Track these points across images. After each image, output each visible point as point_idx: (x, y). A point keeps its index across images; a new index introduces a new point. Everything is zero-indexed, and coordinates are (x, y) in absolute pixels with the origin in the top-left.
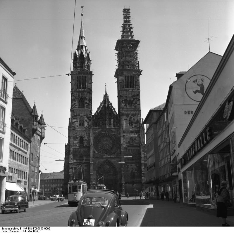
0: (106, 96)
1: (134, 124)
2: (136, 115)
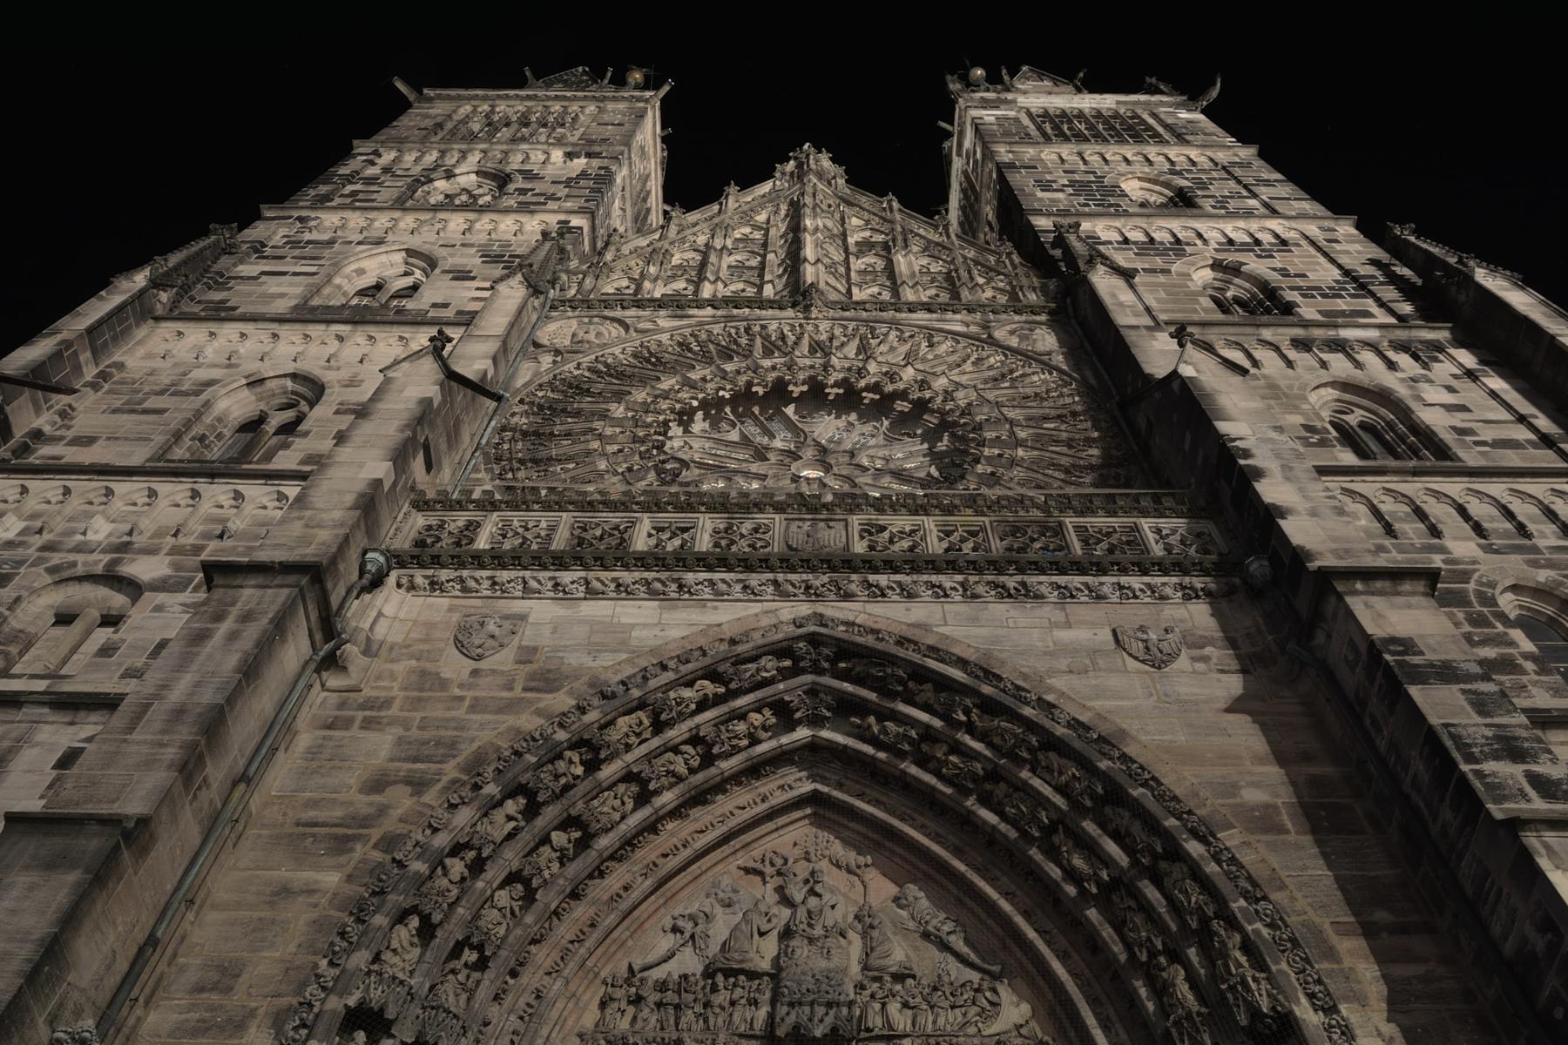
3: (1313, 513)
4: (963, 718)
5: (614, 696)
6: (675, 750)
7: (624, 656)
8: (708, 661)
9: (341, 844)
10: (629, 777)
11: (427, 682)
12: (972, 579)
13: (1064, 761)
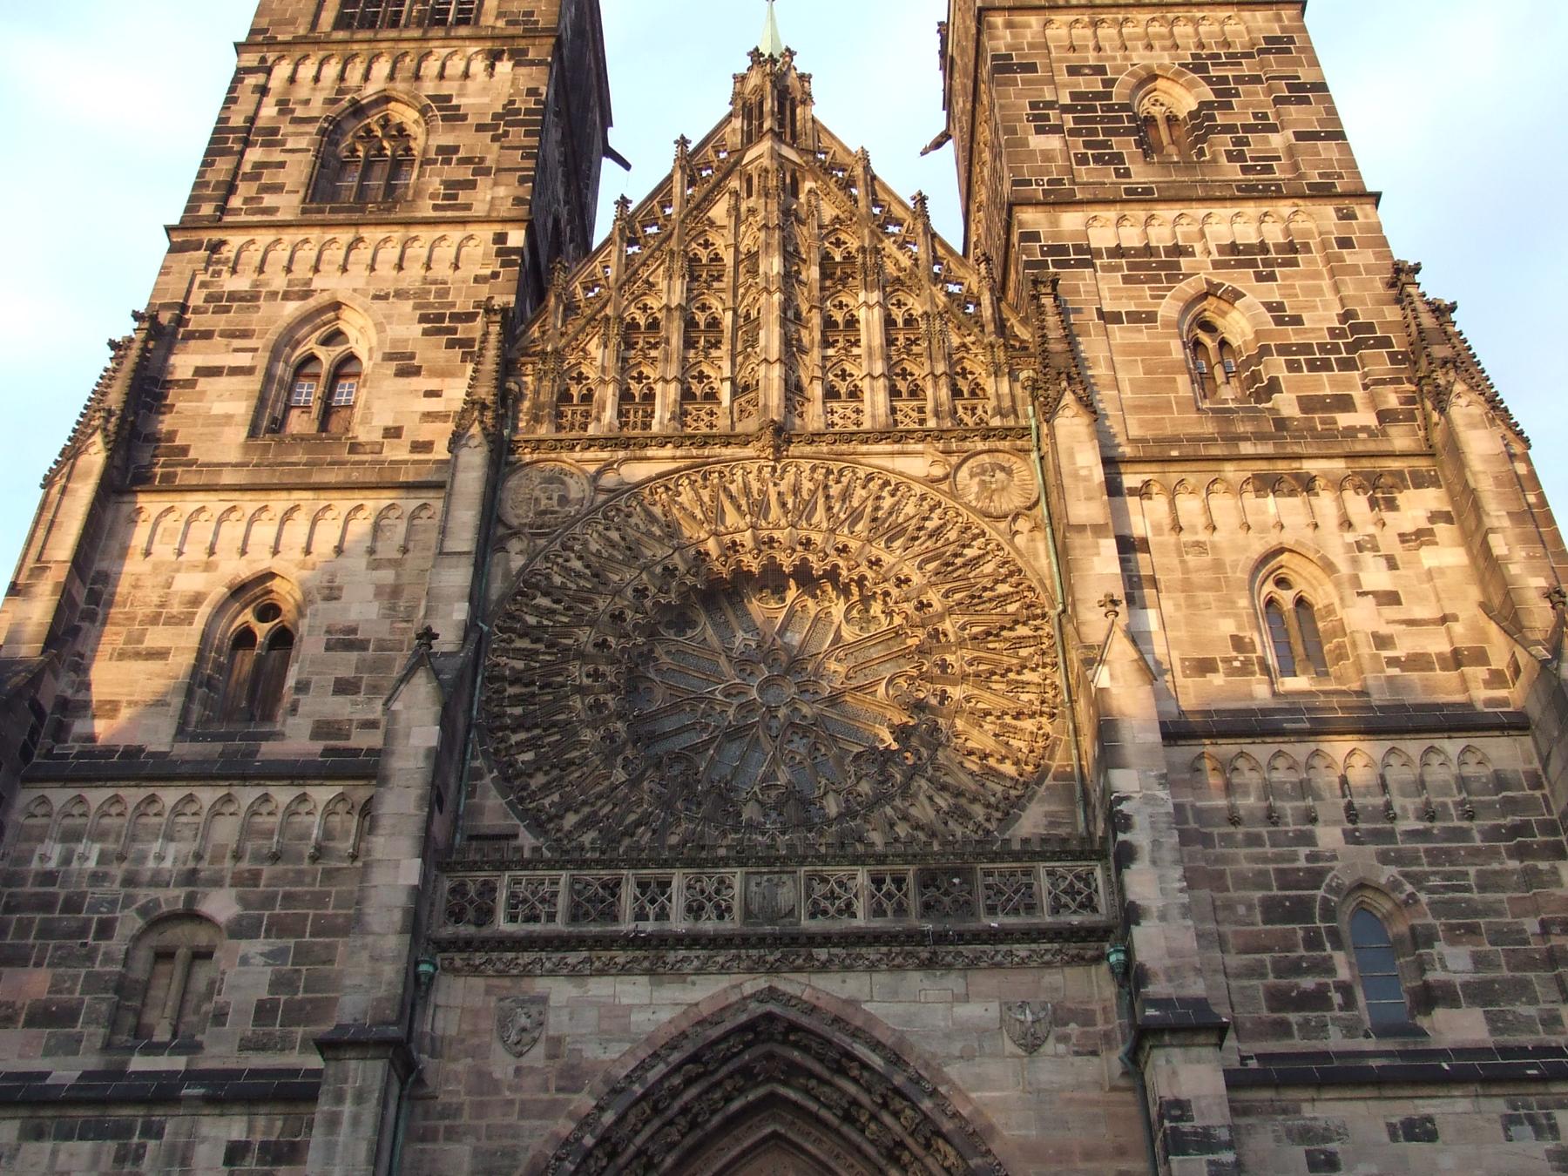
1: (1293, 367)
3: (1163, 917)
4: (880, 1101)
5: (623, 1090)
6: (671, 1123)
7: (627, 1046)
8: (689, 1048)
10: (640, 1153)
11: (483, 1082)
12: (896, 949)
13: (948, 1149)
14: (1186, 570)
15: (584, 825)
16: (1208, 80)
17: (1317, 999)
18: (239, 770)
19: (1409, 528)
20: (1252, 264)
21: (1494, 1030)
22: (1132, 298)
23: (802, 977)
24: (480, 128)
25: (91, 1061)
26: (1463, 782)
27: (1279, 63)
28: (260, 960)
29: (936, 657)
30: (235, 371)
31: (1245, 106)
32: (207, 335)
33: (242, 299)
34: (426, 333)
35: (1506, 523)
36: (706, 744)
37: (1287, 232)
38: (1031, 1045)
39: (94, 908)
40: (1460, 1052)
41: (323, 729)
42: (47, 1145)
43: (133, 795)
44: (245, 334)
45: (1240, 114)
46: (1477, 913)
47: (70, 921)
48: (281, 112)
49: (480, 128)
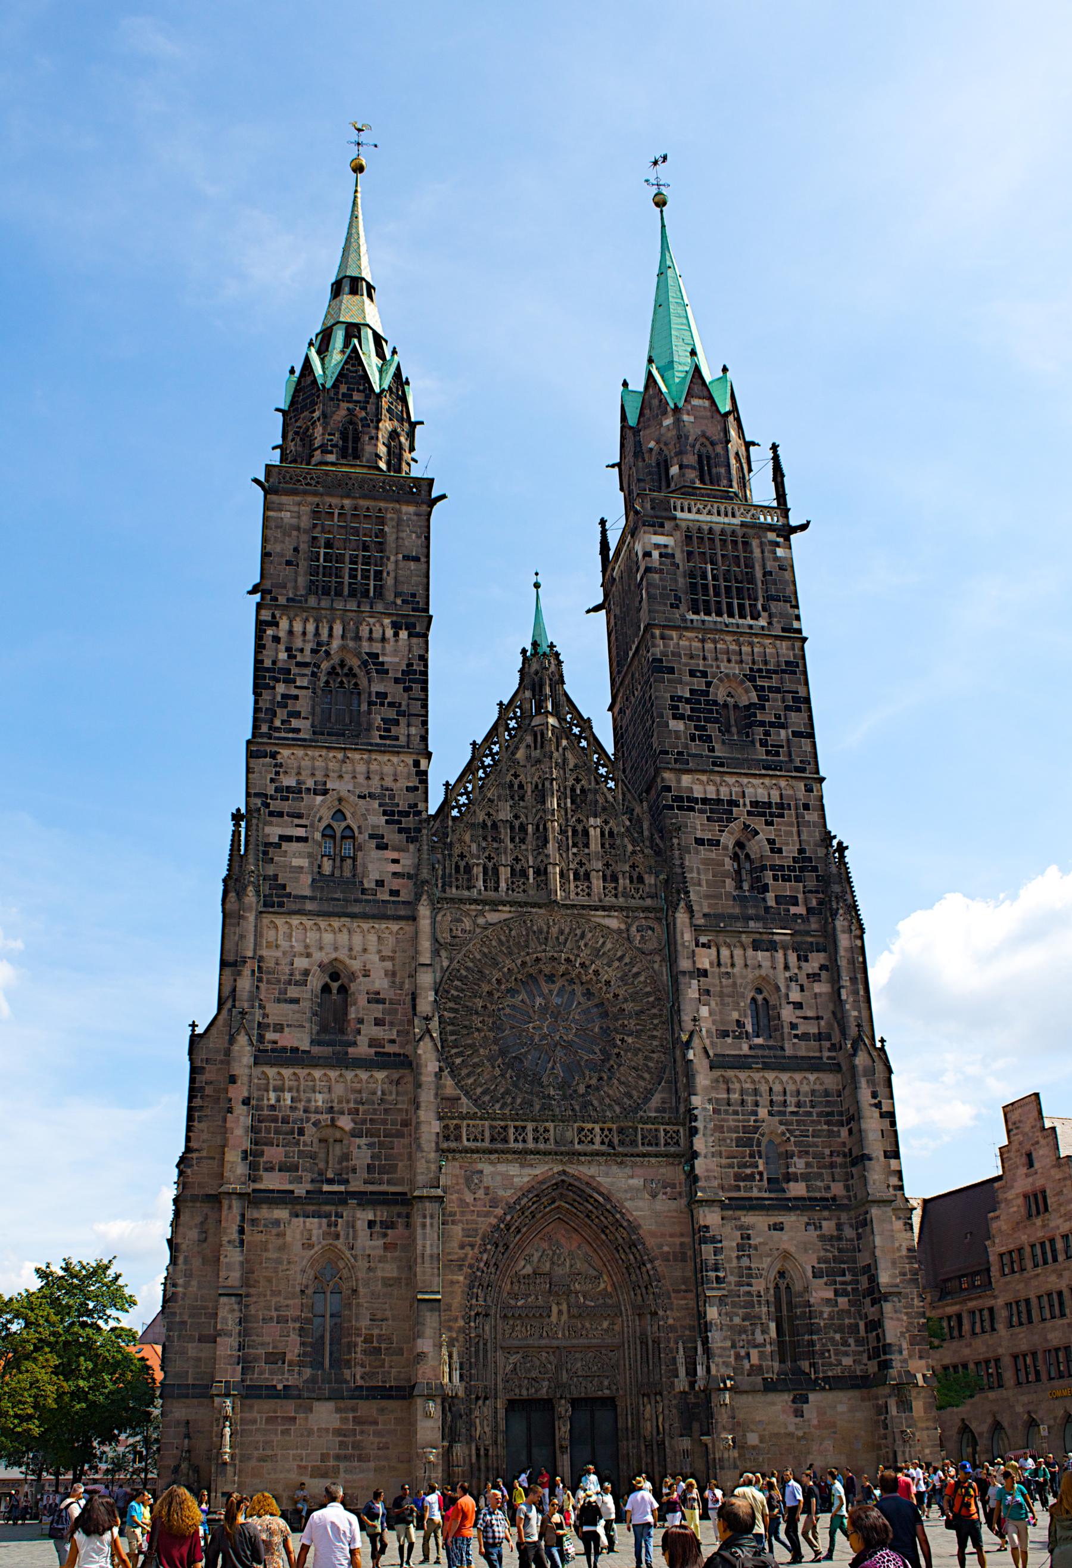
0: (541, 671)
2: (790, 815)
3: (705, 1157)
8: (535, 1193)
9: (460, 1267)
11: (462, 1202)
14: (722, 987)
15: (484, 1093)
16: (755, 687)
17: (750, 1177)
18: (343, 1062)
19: (810, 971)
20: (764, 814)
21: (808, 1191)
22: (710, 831)
23: (575, 1166)
24: (397, 681)
25: (309, 1187)
26: (813, 1092)
27: (790, 682)
28: (365, 1147)
29: (620, 1022)
30: (299, 839)
31: (772, 708)
32: (280, 814)
33: (293, 792)
34: (387, 822)
35: (848, 984)
36: (526, 1052)
37: (781, 795)
38: (654, 1196)
39: (294, 1122)
40: (796, 1199)
41: (373, 1042)
42: (301, 1219)
43: (302, 1072)
44: (299, 816)
45: (766, 716)
46: (810, 1146)
47: (285, 1127)
48: (289, 657)
49: (397, 681)
